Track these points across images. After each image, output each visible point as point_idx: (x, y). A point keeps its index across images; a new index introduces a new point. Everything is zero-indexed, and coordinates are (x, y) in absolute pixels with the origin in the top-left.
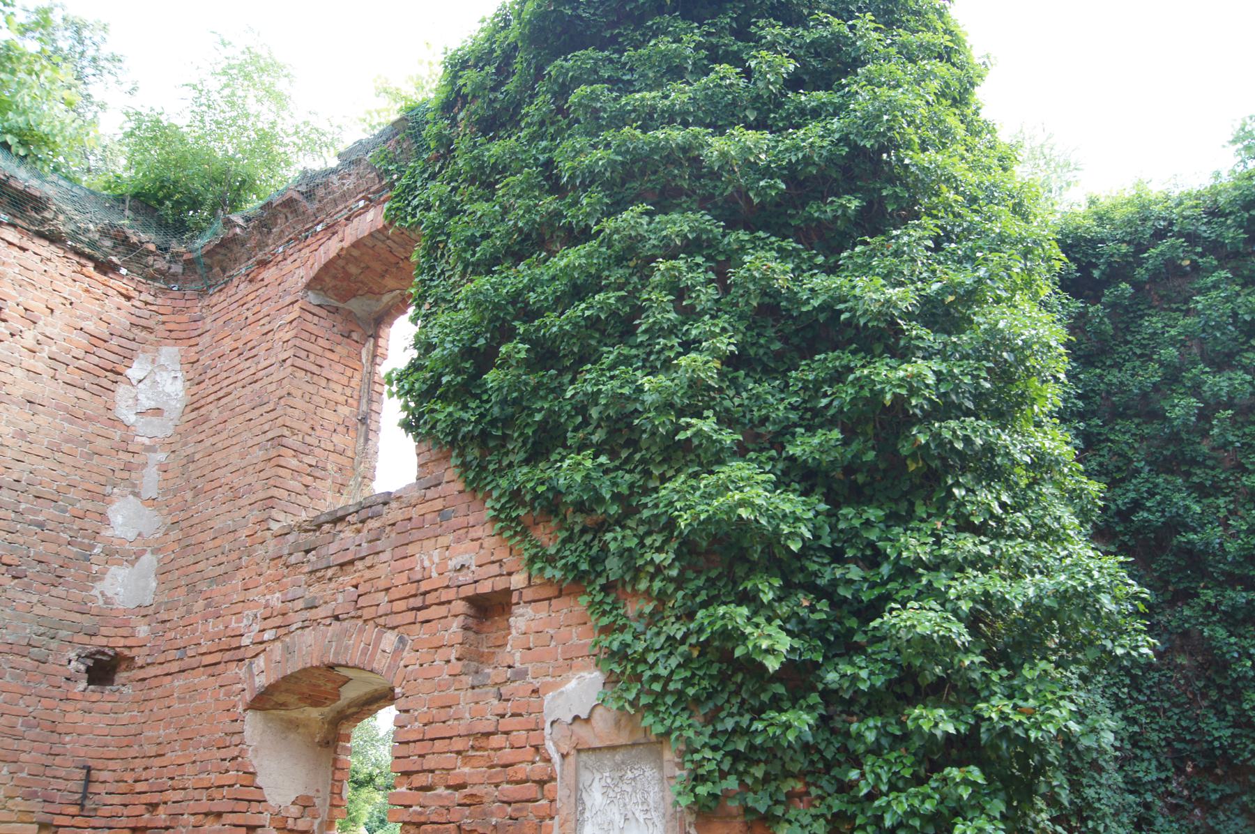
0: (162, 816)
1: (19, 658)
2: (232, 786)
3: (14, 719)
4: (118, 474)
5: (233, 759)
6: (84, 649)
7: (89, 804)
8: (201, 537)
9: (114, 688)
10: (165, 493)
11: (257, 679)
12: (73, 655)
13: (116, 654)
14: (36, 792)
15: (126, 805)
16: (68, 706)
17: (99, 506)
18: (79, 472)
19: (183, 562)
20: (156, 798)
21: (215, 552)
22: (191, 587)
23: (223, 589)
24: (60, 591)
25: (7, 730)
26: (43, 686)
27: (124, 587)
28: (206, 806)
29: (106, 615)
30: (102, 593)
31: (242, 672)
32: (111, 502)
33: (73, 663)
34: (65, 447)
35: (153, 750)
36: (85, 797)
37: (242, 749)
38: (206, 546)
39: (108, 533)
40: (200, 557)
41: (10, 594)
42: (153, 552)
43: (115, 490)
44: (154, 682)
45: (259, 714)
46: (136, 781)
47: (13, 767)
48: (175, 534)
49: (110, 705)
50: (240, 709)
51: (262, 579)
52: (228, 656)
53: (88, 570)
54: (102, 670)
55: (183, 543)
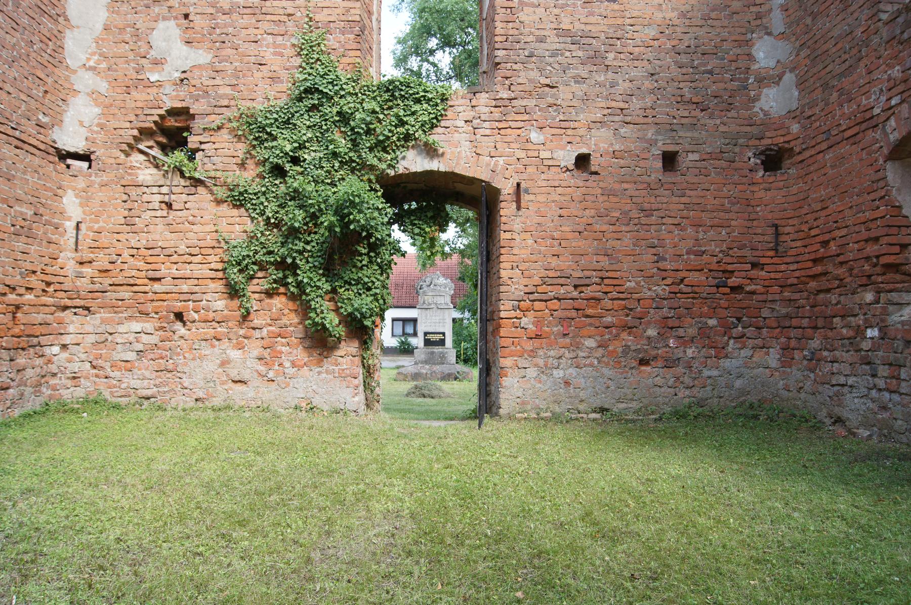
0: (833, 248)
1: (717, 162)
2: (884, 217)
3: (722, 200)
4: (753, 23)
5: (882, 198)
6: (757, 149)
7: (781, 249)
8: (825, 47)
9: (783, 171)
10: (789, 25)
11: (891, 136)
12: (750, 154)
13: (780, 148)
14: (745, 244)
15: (806, 246)
16: (755, 188)
17: (745, 49)
18: (726, 30)
19: (815, 70)
20: (827, 237)
21: (838, 54)
22: (826, 86)
23: (850, 79)
24: (733, 113)
25: (719, 207)
26: (736, 177)
27: (774, 101)
28: (865, 234)
29: (768, 123)
30: (761, 109)
31: (878, 135)
32: (753, 45)
33: (752, 160)
34: (713, 15)
35: (818, 206)
36: (777, 244)
37: (887, 190)
38: (830, 53)
39: (756, 66)
40: (827, 62)
41: (702, 122)
42: (791, 72)
43: (754, 35)
44: (811, 161)
45: (897, 163)
46: (810, 229)
47: (728, 230)
48: (803, 54)
49: (782, 183)
50: (881, 161)
51: (881, 61)
52: (864, 126)
53: (748, 95)
54: (773, 160)
55: (812, 57)
